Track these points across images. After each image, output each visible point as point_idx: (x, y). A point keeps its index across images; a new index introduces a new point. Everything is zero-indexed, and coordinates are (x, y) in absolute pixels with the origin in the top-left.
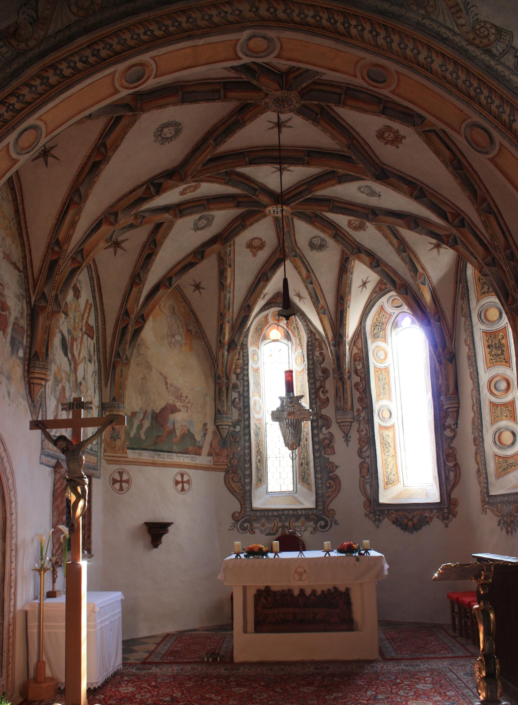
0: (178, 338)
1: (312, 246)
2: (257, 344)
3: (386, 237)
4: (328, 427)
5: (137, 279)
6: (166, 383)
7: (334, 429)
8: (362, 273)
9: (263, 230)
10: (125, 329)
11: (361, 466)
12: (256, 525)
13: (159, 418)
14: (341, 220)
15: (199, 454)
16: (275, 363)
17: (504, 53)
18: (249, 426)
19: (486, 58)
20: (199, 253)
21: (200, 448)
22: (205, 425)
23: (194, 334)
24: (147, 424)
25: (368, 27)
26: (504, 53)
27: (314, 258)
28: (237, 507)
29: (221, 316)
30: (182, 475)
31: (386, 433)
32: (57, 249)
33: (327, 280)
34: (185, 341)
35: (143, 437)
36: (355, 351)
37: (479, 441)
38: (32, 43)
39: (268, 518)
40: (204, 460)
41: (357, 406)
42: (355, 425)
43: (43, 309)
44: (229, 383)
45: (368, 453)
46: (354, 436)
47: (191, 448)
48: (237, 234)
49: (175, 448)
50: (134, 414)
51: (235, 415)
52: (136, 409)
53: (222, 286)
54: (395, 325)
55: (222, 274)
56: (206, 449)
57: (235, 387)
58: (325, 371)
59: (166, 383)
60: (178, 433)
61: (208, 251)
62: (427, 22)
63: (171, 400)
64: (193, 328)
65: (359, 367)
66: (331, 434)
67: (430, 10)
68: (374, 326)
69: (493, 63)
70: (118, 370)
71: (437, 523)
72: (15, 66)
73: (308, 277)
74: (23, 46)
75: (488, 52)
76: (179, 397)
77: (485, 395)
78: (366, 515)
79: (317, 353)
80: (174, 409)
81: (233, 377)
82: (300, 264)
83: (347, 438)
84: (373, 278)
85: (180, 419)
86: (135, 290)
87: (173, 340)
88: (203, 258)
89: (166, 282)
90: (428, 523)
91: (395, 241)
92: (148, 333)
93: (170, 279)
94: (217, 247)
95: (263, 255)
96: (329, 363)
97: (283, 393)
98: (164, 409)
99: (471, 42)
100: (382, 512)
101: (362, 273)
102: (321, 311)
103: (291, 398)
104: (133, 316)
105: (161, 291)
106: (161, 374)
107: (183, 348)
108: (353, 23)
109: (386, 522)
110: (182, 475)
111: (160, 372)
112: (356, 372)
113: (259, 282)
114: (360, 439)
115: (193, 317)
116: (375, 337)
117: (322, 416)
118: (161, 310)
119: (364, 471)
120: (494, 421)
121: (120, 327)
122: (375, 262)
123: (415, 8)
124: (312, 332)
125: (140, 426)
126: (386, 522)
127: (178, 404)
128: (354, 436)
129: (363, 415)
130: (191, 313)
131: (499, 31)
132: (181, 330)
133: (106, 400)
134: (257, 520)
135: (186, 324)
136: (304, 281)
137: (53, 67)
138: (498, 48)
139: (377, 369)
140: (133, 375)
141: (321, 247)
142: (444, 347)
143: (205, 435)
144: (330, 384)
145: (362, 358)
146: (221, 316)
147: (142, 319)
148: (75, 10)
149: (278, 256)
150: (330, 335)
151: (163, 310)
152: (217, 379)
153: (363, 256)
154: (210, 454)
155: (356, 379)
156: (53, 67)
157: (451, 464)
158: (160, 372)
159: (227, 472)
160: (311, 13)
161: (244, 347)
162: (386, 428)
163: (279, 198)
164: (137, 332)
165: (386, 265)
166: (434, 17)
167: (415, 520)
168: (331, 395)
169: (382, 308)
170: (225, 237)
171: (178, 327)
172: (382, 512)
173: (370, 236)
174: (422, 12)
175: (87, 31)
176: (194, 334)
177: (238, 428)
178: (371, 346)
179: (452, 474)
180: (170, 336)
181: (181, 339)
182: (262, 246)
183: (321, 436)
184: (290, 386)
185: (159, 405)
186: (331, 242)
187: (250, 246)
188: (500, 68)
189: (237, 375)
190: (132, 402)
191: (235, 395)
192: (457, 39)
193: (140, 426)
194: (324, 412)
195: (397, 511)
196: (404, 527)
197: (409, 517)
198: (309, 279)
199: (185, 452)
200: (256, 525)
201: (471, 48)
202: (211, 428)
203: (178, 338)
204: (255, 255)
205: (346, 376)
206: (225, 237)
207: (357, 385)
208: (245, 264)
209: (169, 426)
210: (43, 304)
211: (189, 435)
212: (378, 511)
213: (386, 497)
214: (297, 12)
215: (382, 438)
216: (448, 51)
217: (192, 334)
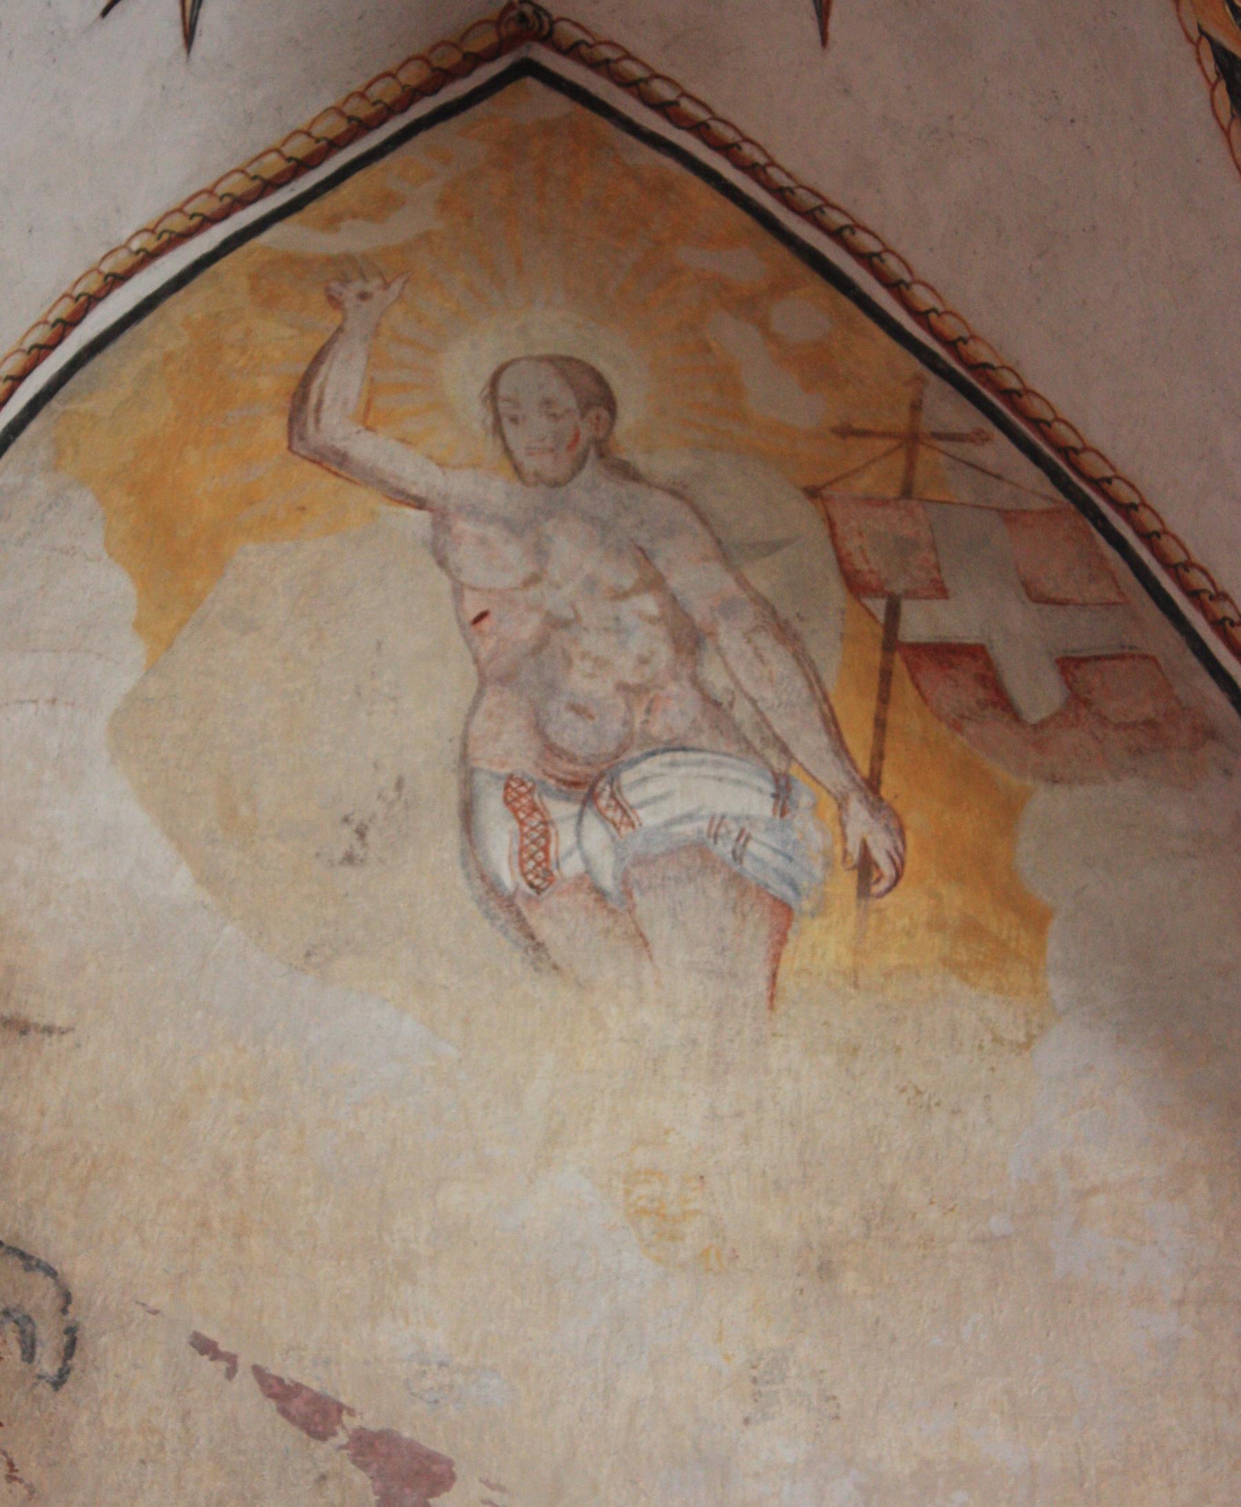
0: (685, 794)
23: (1038, 693)
34: (861, 822)
87: (582, 844)
106: (313, 1414)
107: (823, 942)
111: (281, 1392)
115: (999, 452)
118: (335, 462)
130: (947, 410)
132: (745, 665)
135: (855, 584)
151: (366, 448)
158: (281, 1392)
171: (690, 640)
176: (1038, 693)
180: (516, 792)
181: (761, 805)
203: (685, 794)
217: (999, 699)
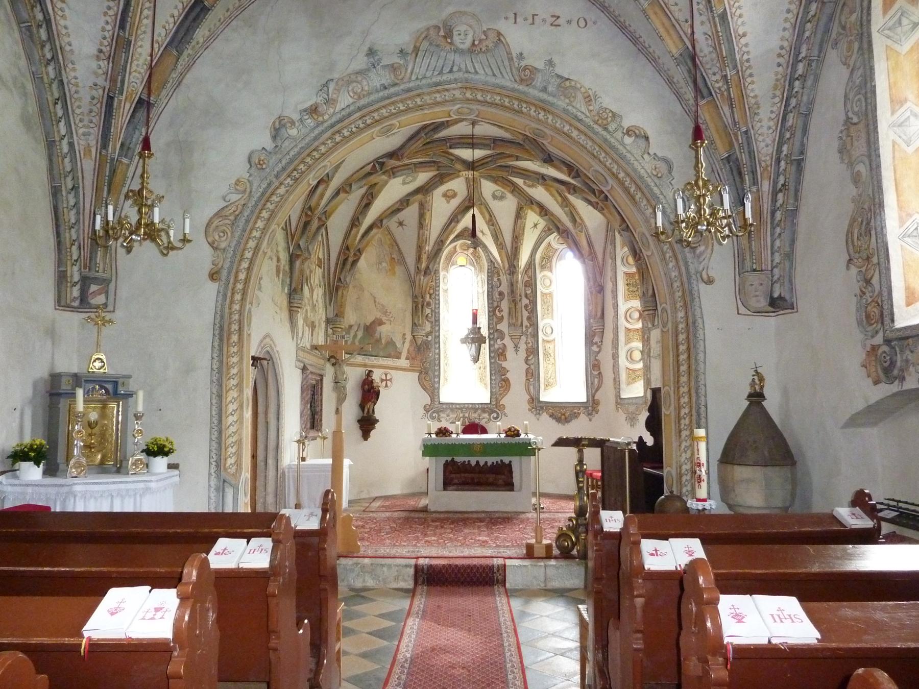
0: (384, 264)
1: (495, 197)
2: (446, 269)
3: (553, 196)
4: (502, 339)
5: (355, 222)
6: (375, 302)
7: (507, 341)
8: (532, 217)
9: (458, 185)
10: (346, 260)
11: (527, 371)
12: (442, 415)
13: (370, 329)
14: (519, 182)
15: (398, 357)
16: (462, 290)
17: (616, 130)
18: (439, 336)
19: (604, 133)
20: (404, 202)
21: (400, 353)
22: (404, 334)
24: (360, 334)
25: (533, 109)
26: (616, 130)
27: (494, 205)
28: (428, 401)
29: (420, 248)
30: (386, 375)
31: (548, 345)
32: (309, 213)
33: (506, 223)
35: (357, 344)
36: (526, 279)
37: (615, 357)
38: (326, 117)
39: (452, 410)
40: (403, 362)
41: (525, 323)
42: (524, 338)
43: (298, 256)
44: (424, 303)
45: (532, 362)
46: (522, 346)
47: (393, 354)
48: (437, 187)
49: (381, 354)
50: (351, 327)
51: (428, 327)
52: (352, 323)
53: (421, 226)
54: (560, 258)
55: (422, 216)
56: (404, 354)
57: (429, 304)
58: (501, 294)
59: (375, 302)
60: (383, 341)
61: (412, 199)
62: (570, 108)
63: (378, 315)
64: (396, 257)
65: (528, 292)
66: (505, 345)
67: (572, 99)
68: (543, 258)
69: (608, 137)
70: (340, 293)
71: (583, 418)
72: (317, 132)
73: (491, 220)
74: (320, 119)
75: (606, 129)
76: (385, 313)
77: (622, 323)
78: (530, 410)
79: (495, 279)
80: (381, 323)
81: (428, 298)
82: (484, 210)
83: (516, 347)
84: (542, 223)
85: (384, 330)
86: (354, 230)
88: (408, 205)
89: (378, 223)
90: (576, 417)
91: (559, 199)
92: (362, 263)
93: (381, 221)
94: (419, 197)
95: (455, 203)
96: (504, 288)
97: (470, 326)
98: (373, 322)
99: (596, 122)
100: (542, 408)
101: (532, 217)
102: (500, 246)
103: (476, 330)
104: (352, 251)
105: (375, 231)
108: (524, 105)
109: (545, 416)
110: (386, 375)
112: (526, 296)
113: (450, 223)
114: (527, 350)
116: (543, 267)
117: (497, 330)
119: (529, 375)
120: (628, 341)
121: (342, 258)
122: (543, 211)
123: (562, 98)
124: (491, 262)
125: (355, 336)
126: (545, 416)
127: (384, 319)
128: (522, 346)
129: (530, 330)
131: (614, 115)
133: (331, 316)
134: (443, 411)
136: (487, 223)
137: (339, 132)
138: (611, 127)
139: (543, 294)
140: (351, 296)
141: (502, 198)
142: (595, 281)
143: (404, 343)
144: (505, 305)
145: (531, 284)
146: (420, 248)
147: (360, 252)
148: (352, 94)
149: (467, 204)
150: (507, 266)
152: (414, 297)
153: (535, 207)
154: (407, 358)
155: (525, 301)
156: (339, 132)
157: (596, 373)
159: (421, 373)
160: (498, 98)
161: (437, 272)
162: (548, 342)
163: (471, 166)
164: (355, 262)
165: (552, 215)
166: (574, 104)
167: (567, 415)
168: (505, 313)
169: (549, 244)
170: (425, 190)
172: (542, 408)
173: (539, 193)
174: (567, 101)
175: (360, 109)
177: (430, 338)
178: (539, 276)
179: (596, 381)
182: (455, 195)
183: (496, 346)
184: (475, 321)
185: (370, 319)
186: (509, 195)
187: (445, 195)
188: (613, 140)
189: (431, 295)
190: (351, 317)
191: (428, 311)
192: (587, 120)
193: (355, 336)
194: (499, 327)
195: (553, 407)
196: (559, 420)
197: (562, 413)
198: (491, 221)
199: (389, 356)
200: (442, 415)
201: (595, 126)
202: (409, 337)
204: (448, 202)
205: (518, 299)
206: (425, 190)
207: (526, 306)
208: (441, 208)
209: (377, 335)
210: (299, 253)
211: (391, 343)
212: (537, 406)
213: (546, 396)
214: (489, 97)
215: (545, 350)
216: (582, 128)
